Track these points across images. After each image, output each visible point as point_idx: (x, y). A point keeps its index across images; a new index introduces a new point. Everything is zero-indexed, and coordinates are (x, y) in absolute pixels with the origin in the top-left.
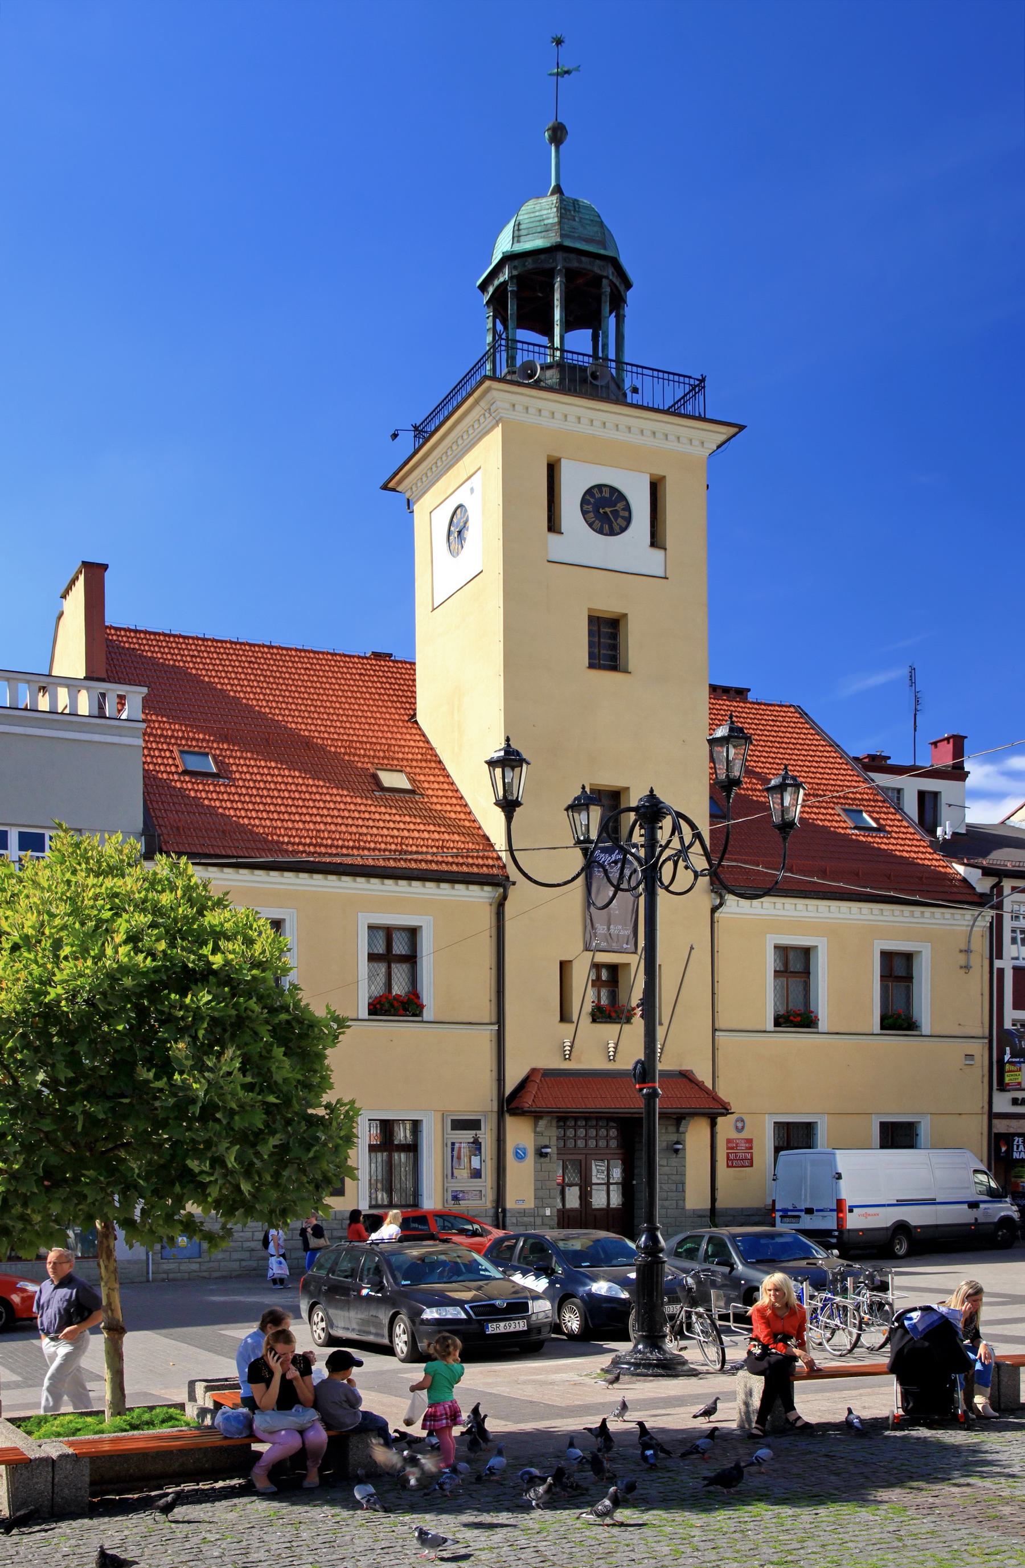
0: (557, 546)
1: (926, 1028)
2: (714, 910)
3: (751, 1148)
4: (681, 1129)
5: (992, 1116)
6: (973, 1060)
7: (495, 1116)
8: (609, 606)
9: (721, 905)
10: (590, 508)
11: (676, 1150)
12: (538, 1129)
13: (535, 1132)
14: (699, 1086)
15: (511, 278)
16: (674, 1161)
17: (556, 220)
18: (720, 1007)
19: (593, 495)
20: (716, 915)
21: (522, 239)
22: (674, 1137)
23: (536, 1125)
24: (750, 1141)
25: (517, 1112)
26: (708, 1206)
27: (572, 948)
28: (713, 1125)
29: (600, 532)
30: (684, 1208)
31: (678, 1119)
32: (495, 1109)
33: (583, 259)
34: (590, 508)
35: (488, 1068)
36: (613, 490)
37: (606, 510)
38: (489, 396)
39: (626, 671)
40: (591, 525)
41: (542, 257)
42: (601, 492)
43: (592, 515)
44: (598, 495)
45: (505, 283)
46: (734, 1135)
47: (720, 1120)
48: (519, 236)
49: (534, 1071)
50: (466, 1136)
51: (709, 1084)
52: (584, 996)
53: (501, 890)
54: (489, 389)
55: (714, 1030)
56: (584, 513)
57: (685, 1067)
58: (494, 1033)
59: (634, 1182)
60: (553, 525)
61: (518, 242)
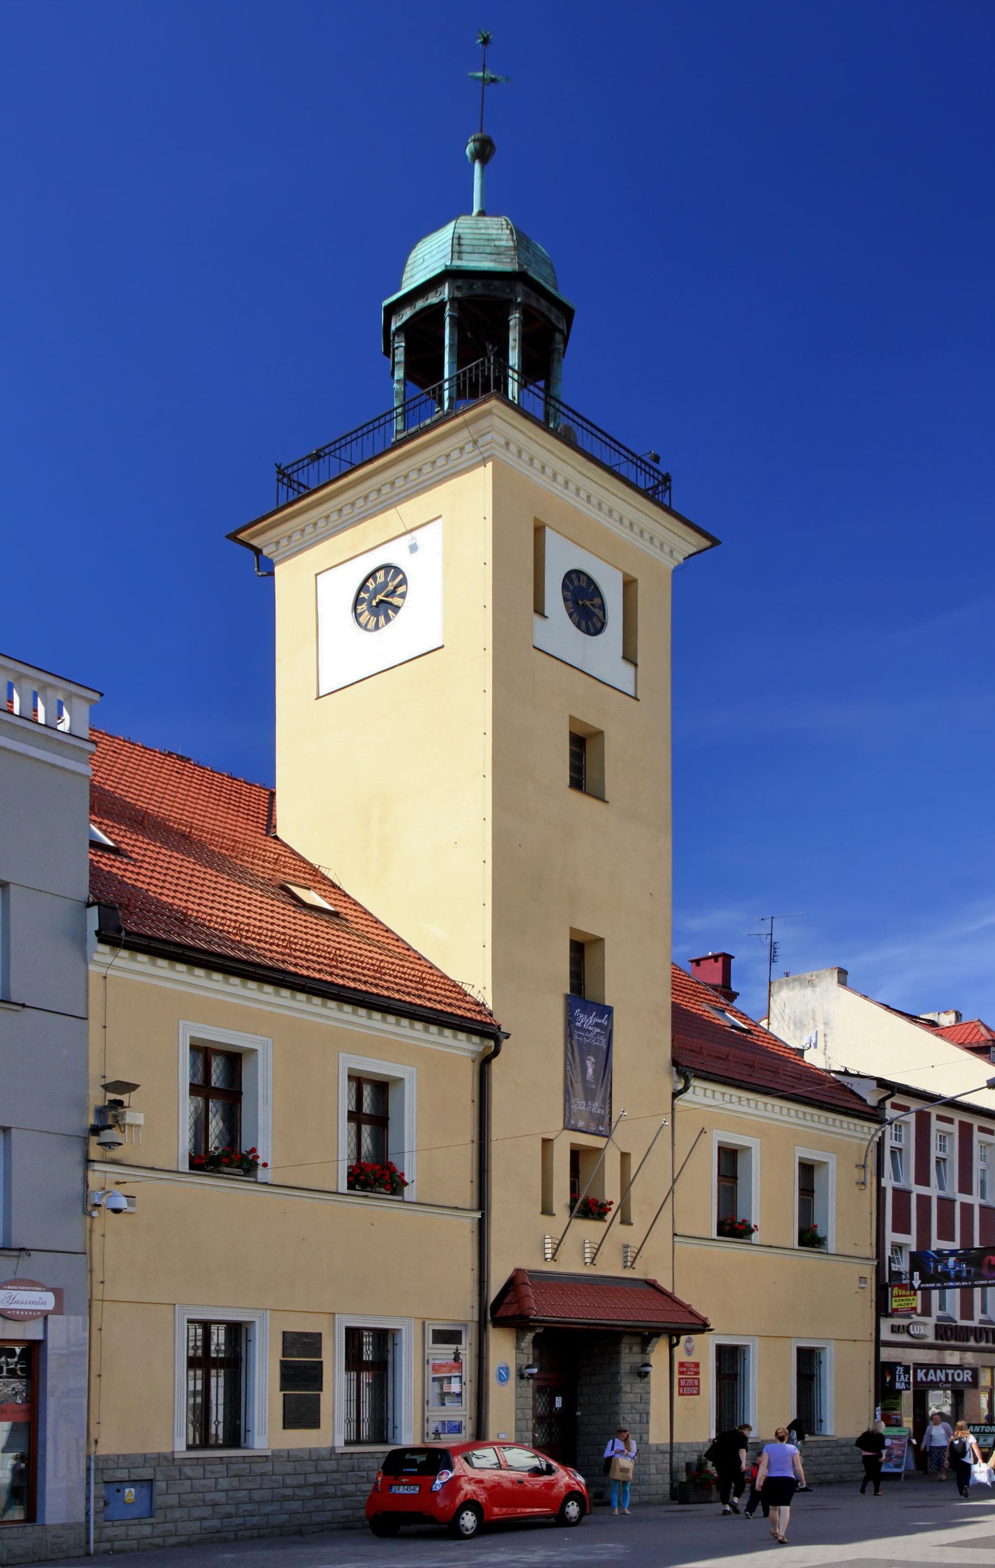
1: (832, 1246)
3: (697, 1373)
4: (649, 1348)
5: (879, 1344)
6: (865, 1283)
11: (642, 1374)
12: (523, 1345)
13: (518, 1347)
15: (452, 299)
16: (639, 1386)
21: (465, 256)
22: (638, 1359)
23: (519, 1340)
24: (697, 1365)
25: (500, 1323)
26: (668, 1441)
27: (553, 1124)
30: (647, 1443)
31: (645, 1337)
35: (470, 1267)
41: (497, 283)
45: (442, 304)
46: (685, 1359)
48: (460, 252)
49: (518, 1271)
50: (445, 1352)
53: (492, 1043)
57: (650, 1277)
58: (476, 1221)
59: (579, 1413)
61: (460, 258)
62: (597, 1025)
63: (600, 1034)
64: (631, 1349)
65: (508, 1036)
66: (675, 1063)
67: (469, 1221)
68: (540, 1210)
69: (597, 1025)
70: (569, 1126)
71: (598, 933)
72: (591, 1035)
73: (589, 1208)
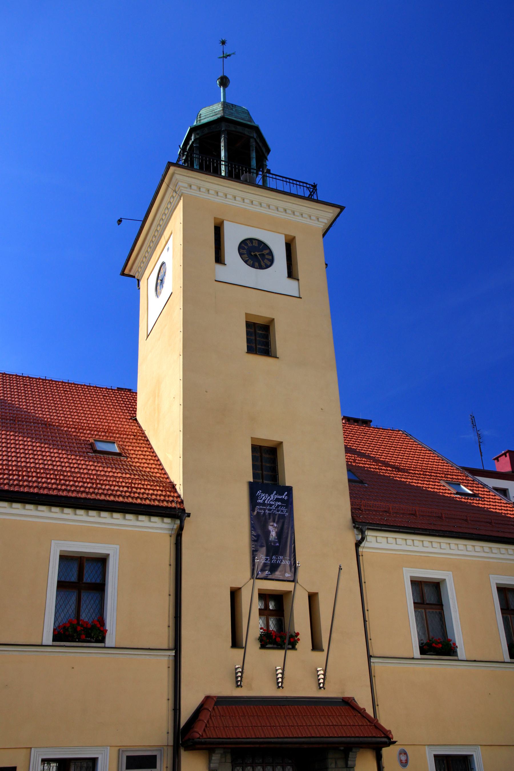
0: (221, 272)
2: (358, 544)
4: (350, 763)
7: (170, 751)
8: (262, 311)
9: (363, 539)
10: (245, 251)
14: (361, 713)
17: (221, 109)
18: (372, 635)
19: (246, 244)
20: (360, 549)
28: (379, 758)
29: (253, 266)
32: (171, 743)
33: (238, 127)
34: (245, 251)
36: (260, 242)
37: (256, 254)
38: (174, 180)
39: (276, 357)
40: (246, 262)
42: (252, 243)
43: (246, 256)
44: (250, 245)
47: (385, 751)
51: (370, 712)
52: (254, 625)
54: (173, 174)
55: (369, 657)
56: (241, 254)
60: (219, 259)
62: (277, 500)
63: (281, 506)
64: (336, 763)
65: (189, 515)
66: (354, 520)
67: (166, 658)
68: (230, 644)
69: (277, 500)
70: (254, 576)
71: (276, 438)
72: (273, 507)
73: (278, 638)
